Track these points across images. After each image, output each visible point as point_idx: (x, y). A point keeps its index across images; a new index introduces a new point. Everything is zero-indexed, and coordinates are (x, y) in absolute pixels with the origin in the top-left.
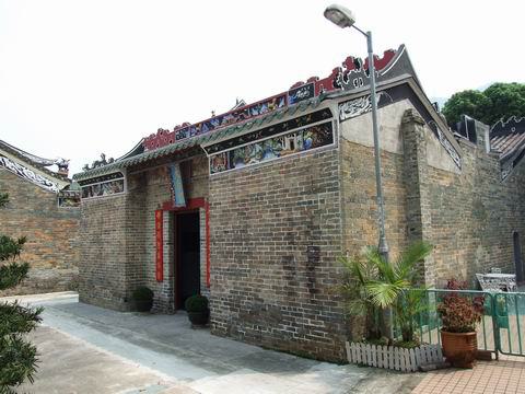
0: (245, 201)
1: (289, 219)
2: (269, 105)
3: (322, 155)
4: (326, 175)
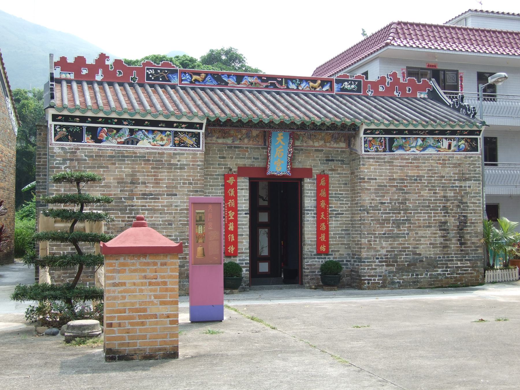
0: (403, 179)
1: (444, 197)
2: (311, 84)
3: (471, 157)
4: (472, 171)
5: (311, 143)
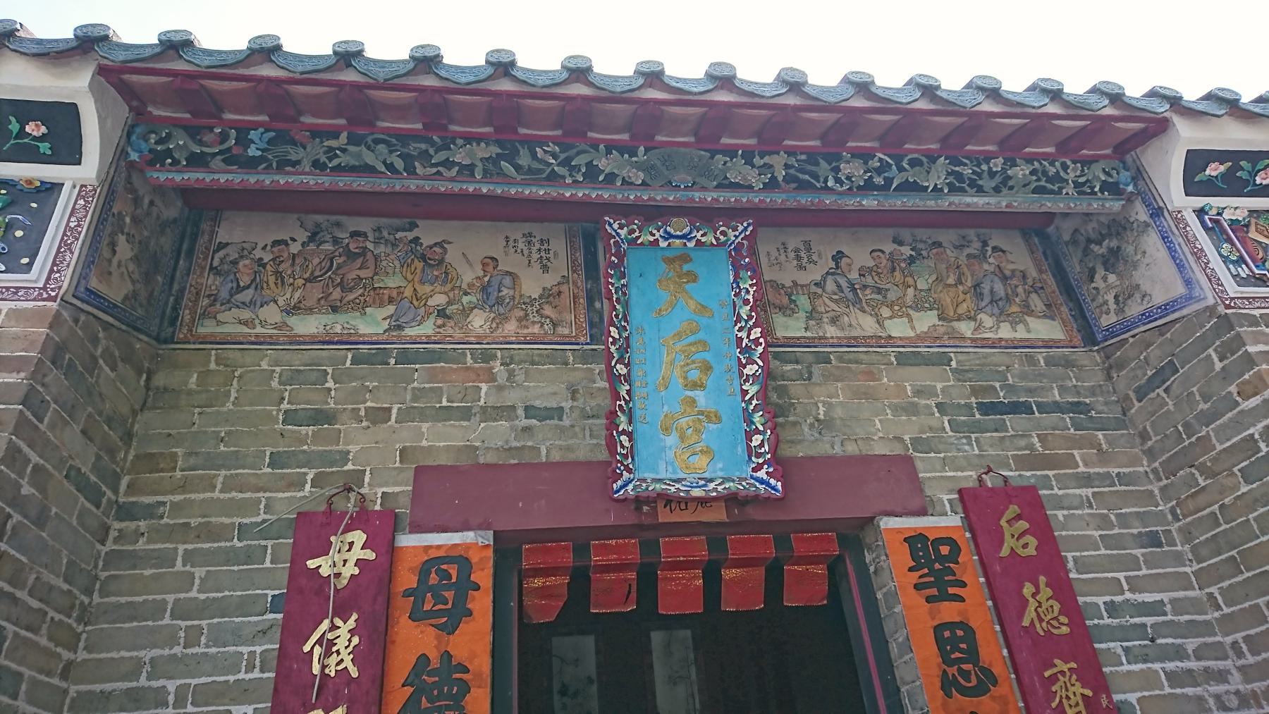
5: (866, 324)
